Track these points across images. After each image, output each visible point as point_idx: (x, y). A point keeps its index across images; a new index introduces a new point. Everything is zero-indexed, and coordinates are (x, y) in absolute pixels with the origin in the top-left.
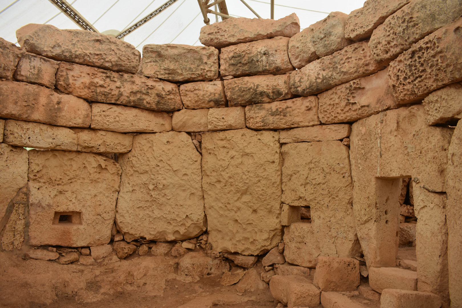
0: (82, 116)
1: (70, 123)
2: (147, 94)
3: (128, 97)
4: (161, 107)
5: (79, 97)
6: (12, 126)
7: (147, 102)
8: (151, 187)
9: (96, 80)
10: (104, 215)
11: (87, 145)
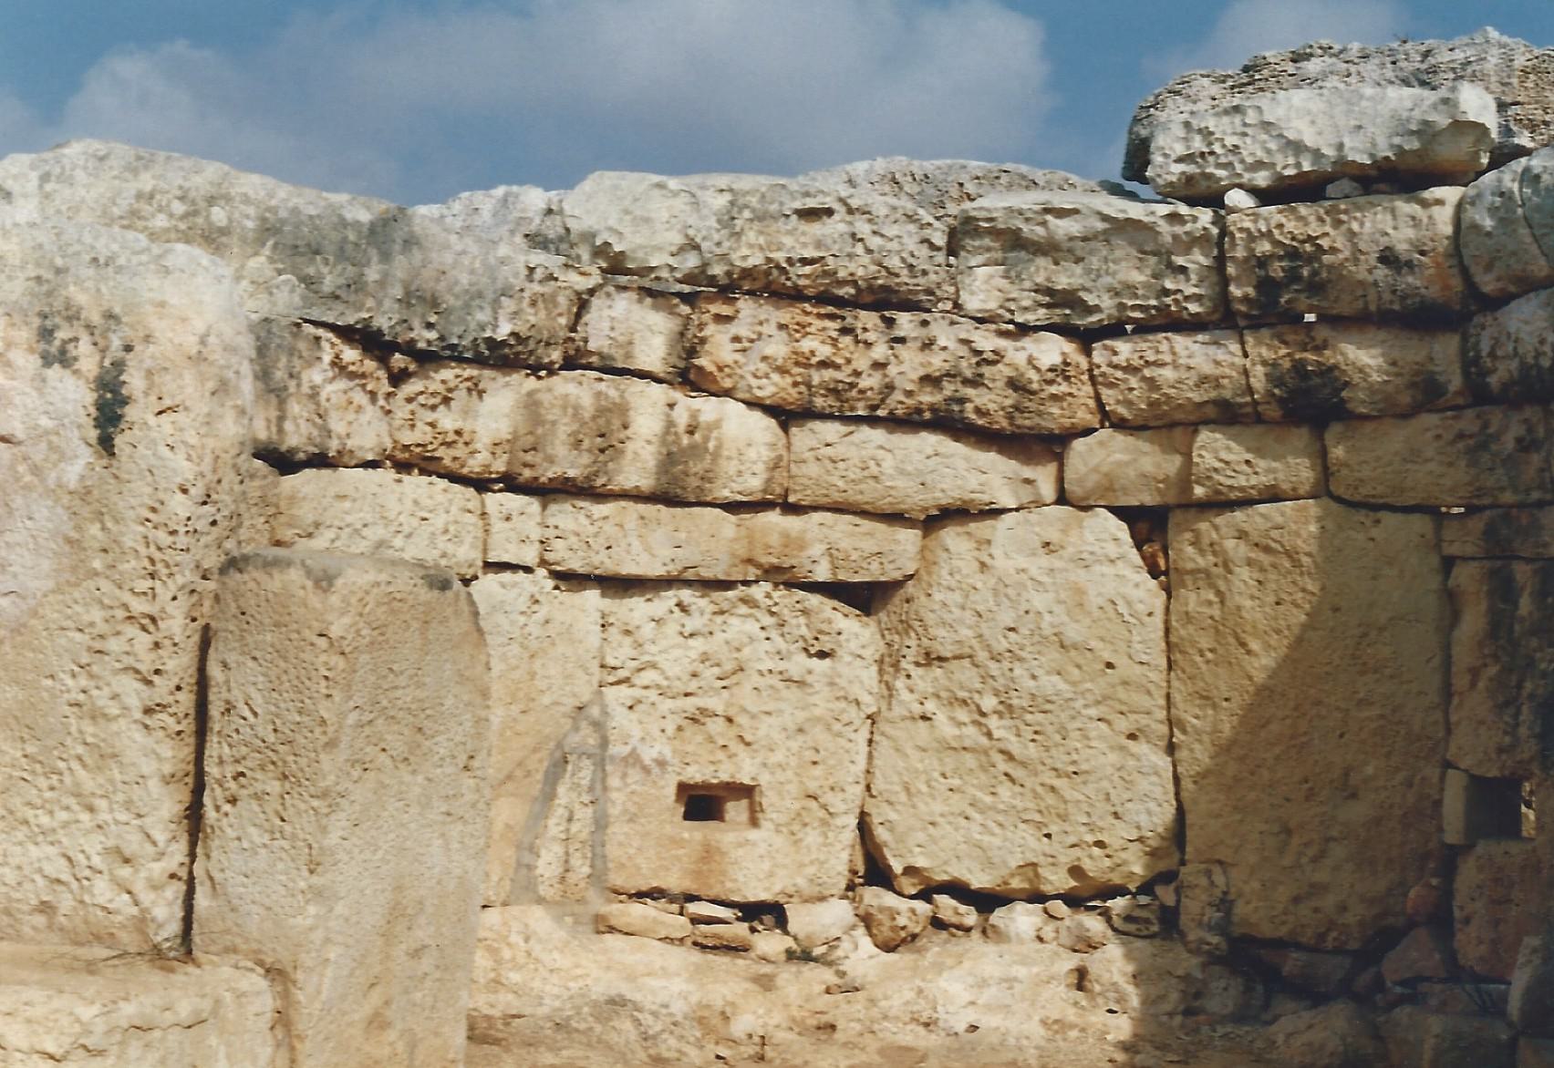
0: (760, 468)
1: (726, 493)
2: (976, 382)
3: (909, 394)
4: (1024, 421)
5: (752, 404)
6: (567, 515)
7: (978, 411)
8: (989, 703)
9: (807, 345)
10: (828, 798)
11: (775, 561)
